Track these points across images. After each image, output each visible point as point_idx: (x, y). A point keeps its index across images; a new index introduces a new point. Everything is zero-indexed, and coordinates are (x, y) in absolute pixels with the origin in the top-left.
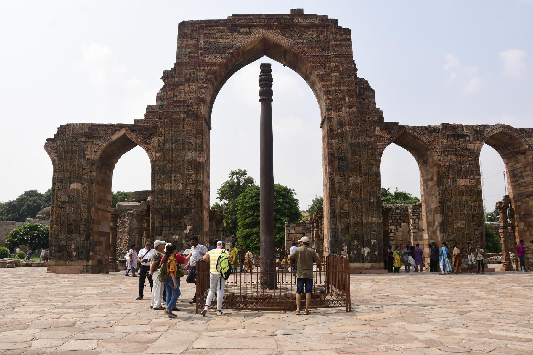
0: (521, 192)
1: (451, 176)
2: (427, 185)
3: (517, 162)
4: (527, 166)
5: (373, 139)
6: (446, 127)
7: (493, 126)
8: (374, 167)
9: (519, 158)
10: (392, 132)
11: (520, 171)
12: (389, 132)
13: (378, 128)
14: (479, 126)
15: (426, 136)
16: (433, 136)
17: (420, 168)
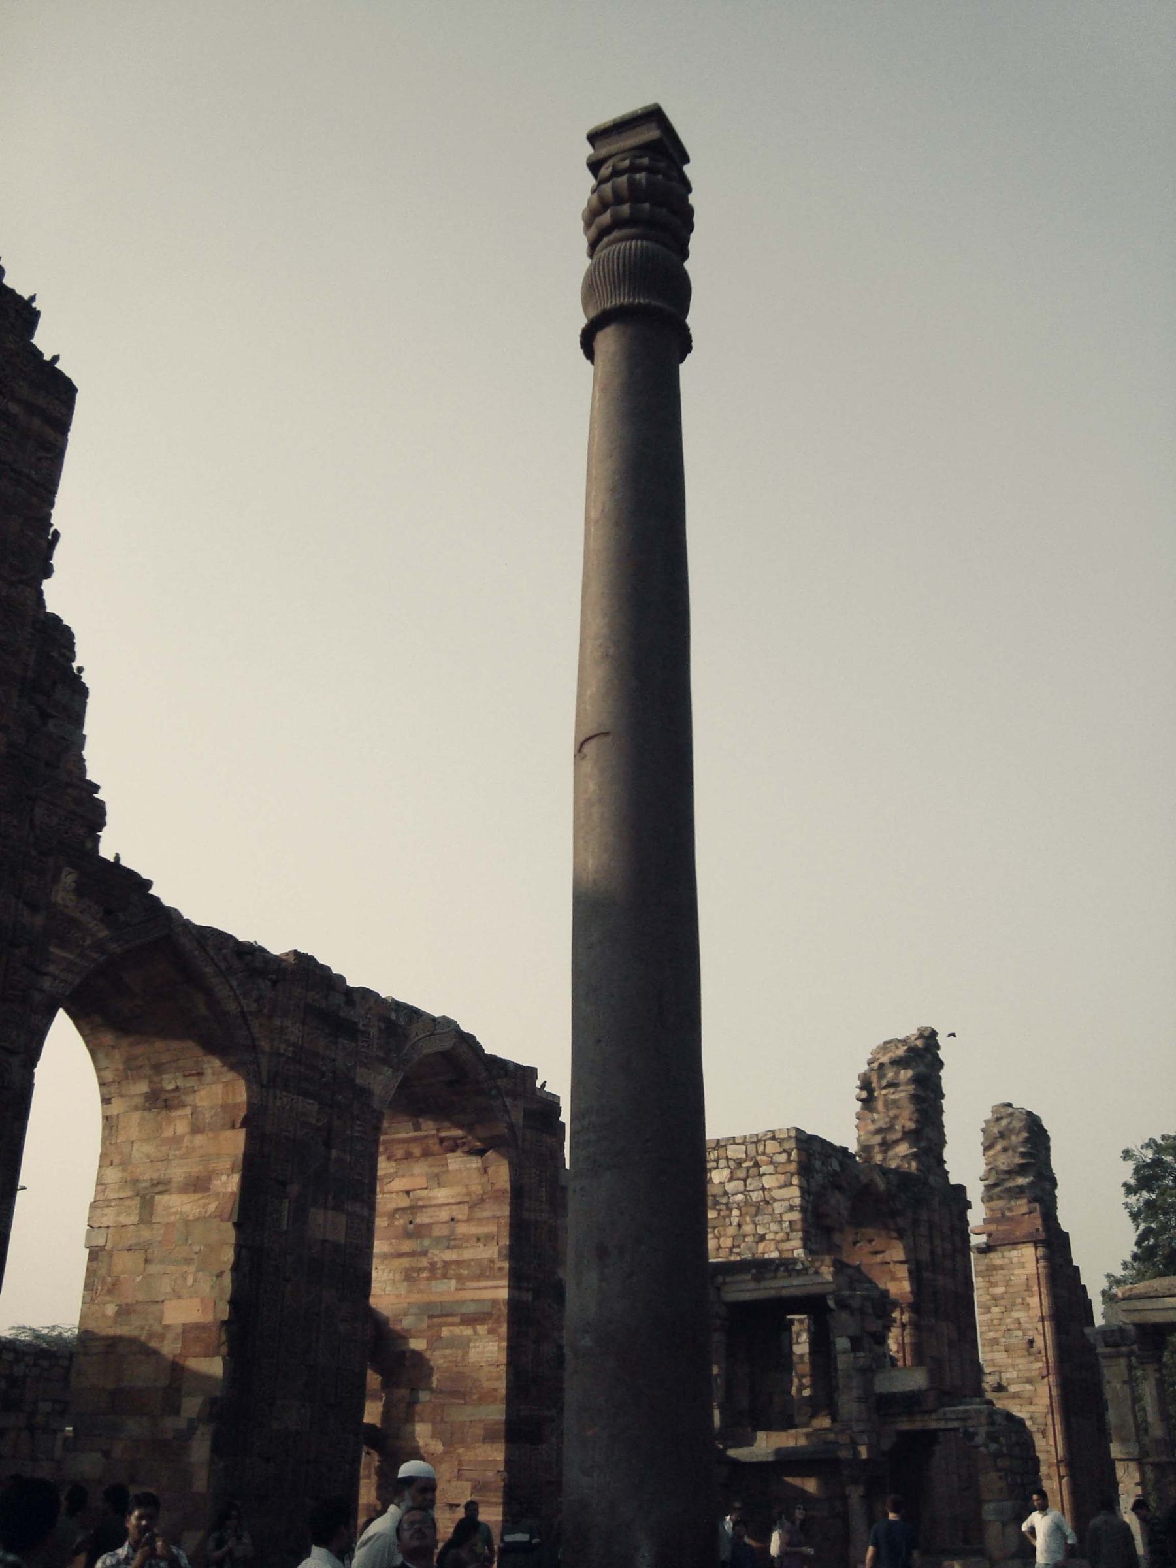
0: (434, 1298)
1: (294, 1189)
2: (147, 1206)
3: (438, 1180)
4: (482, 1200)
5: (39, 920)
6: (304, 969)
7: (434, 1019)
8: (16, 1061)
9: (450, 1168)
10: (122, 917)
11: (444, 1215)
12: (108, 912)
13: (69, 878)
14: (398, 1004)
15: (234, 983)
16: (255, 994)
17: (106, 1118)
